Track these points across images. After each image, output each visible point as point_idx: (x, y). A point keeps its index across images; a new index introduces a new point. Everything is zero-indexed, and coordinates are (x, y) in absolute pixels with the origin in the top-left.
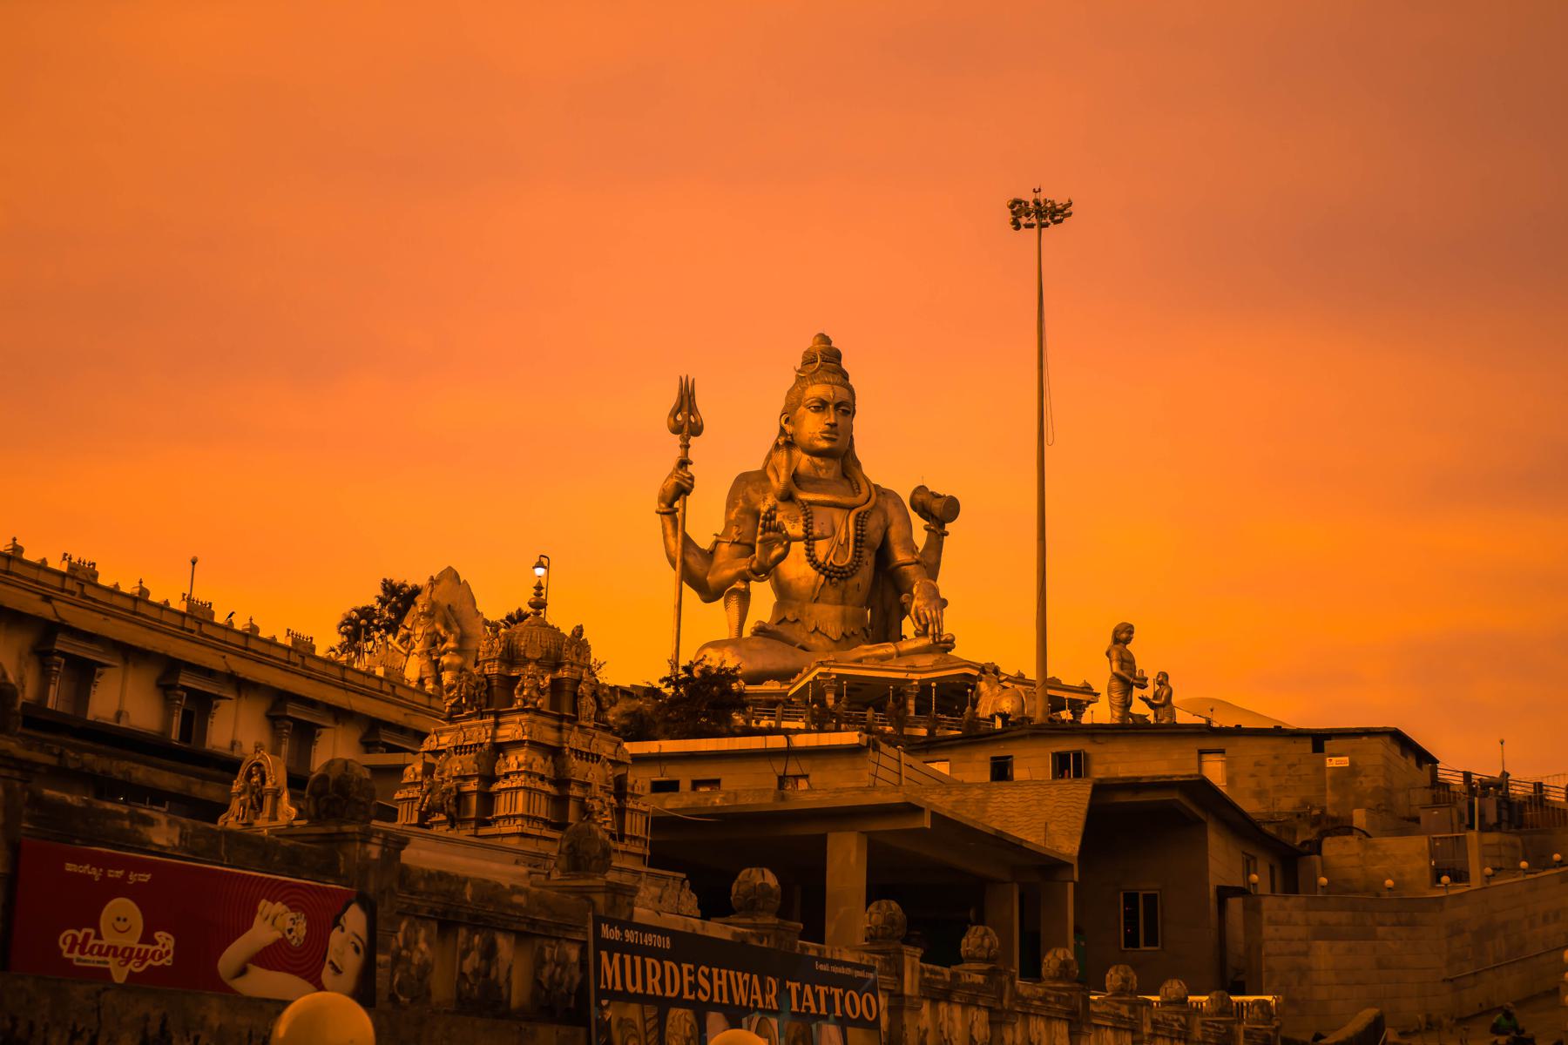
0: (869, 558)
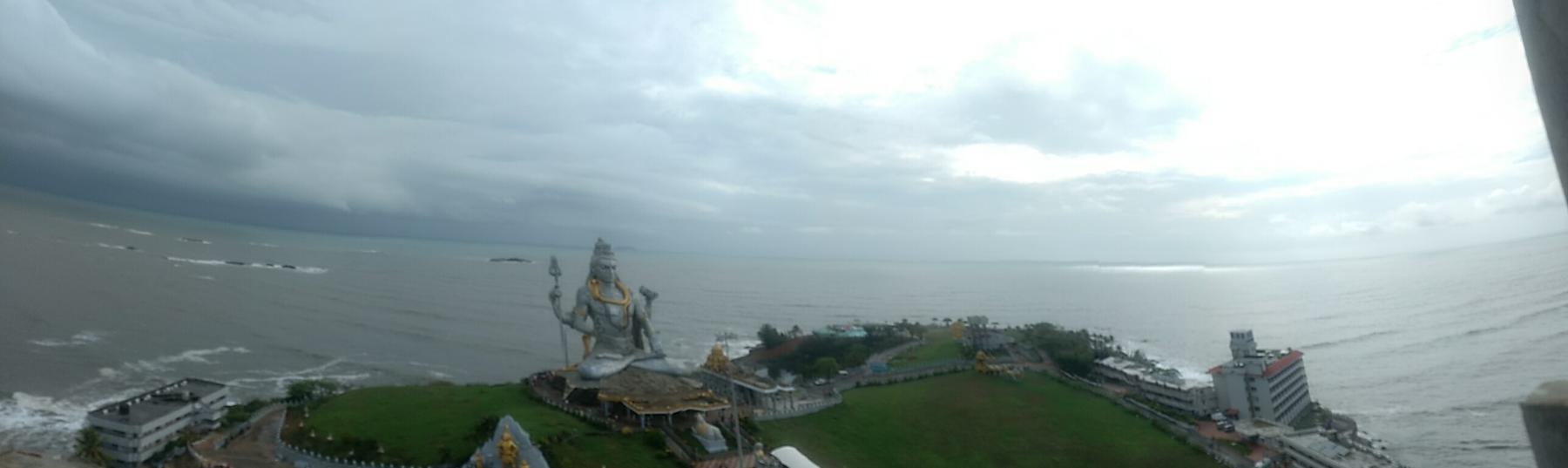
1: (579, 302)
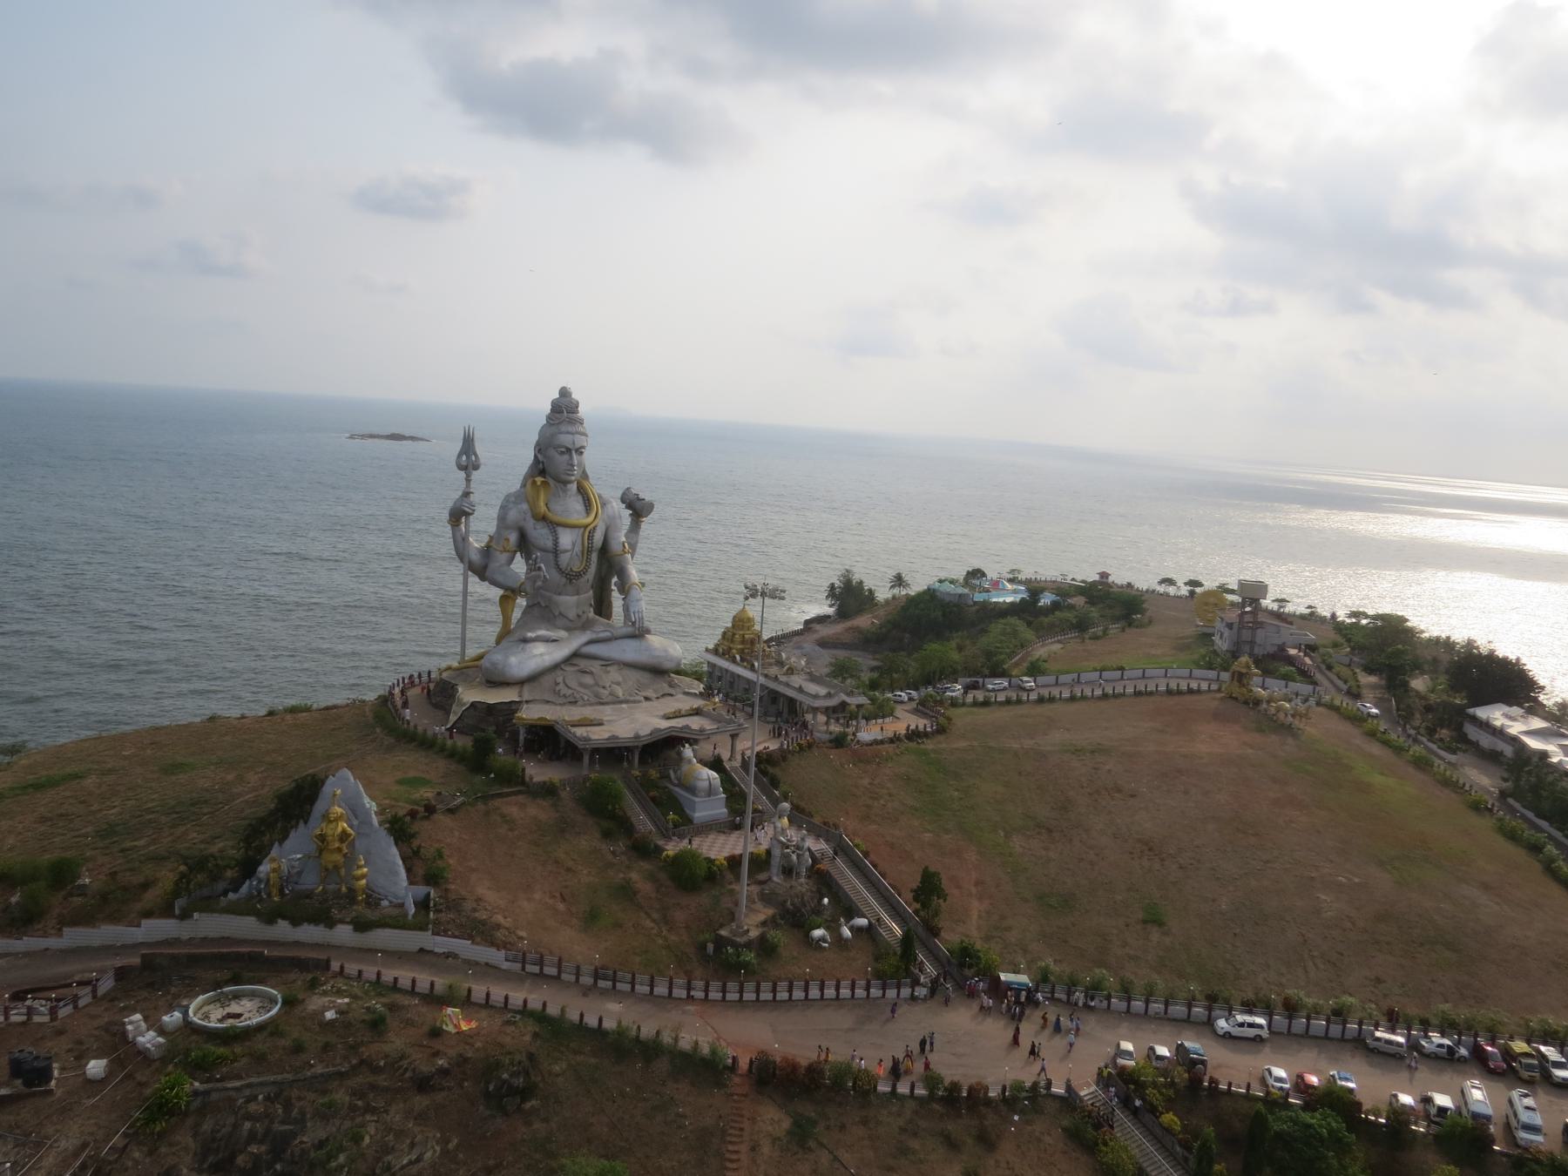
0: (594, 557)
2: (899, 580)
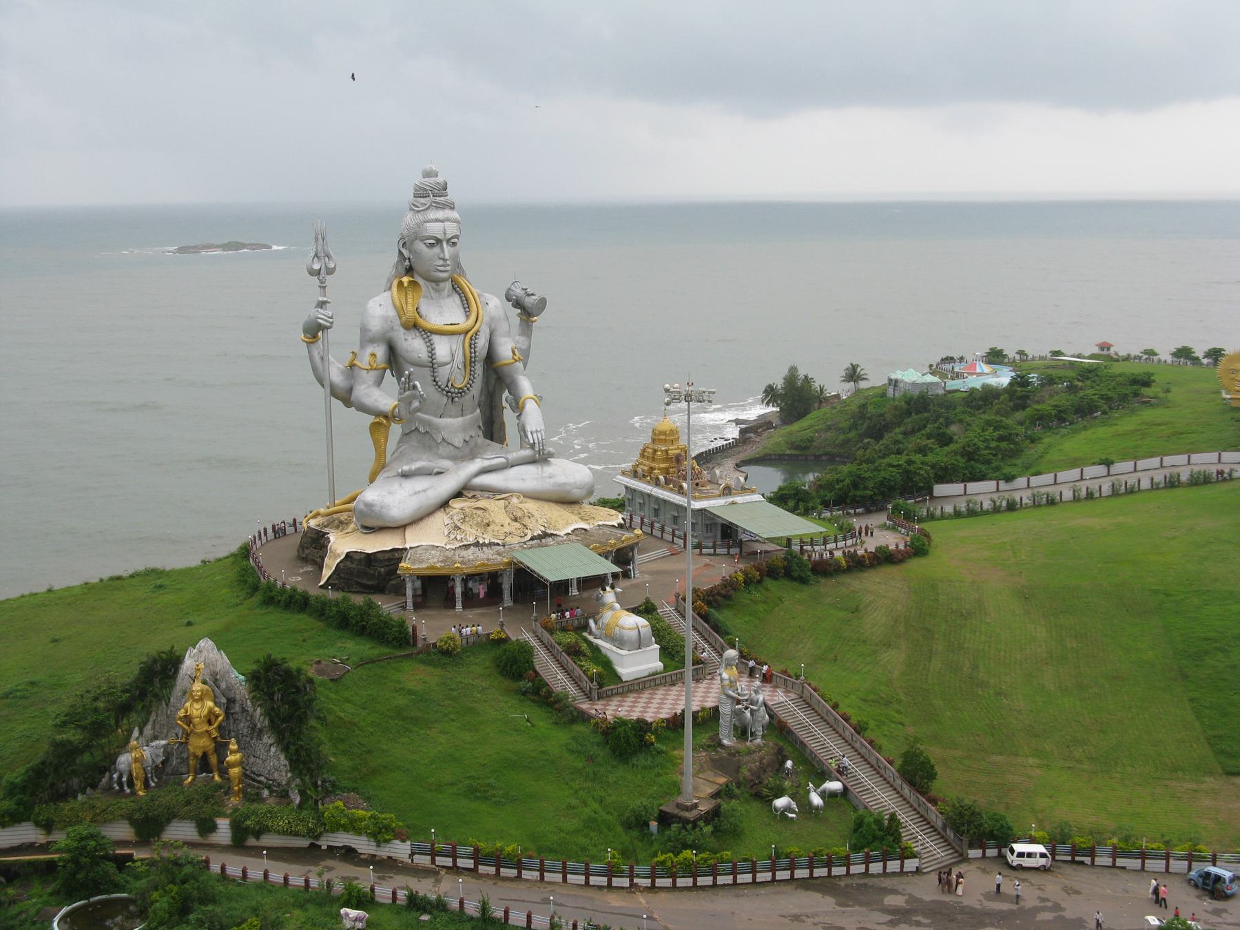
0: (479, 369)
1: (367, 338)
2: (853, 375)
